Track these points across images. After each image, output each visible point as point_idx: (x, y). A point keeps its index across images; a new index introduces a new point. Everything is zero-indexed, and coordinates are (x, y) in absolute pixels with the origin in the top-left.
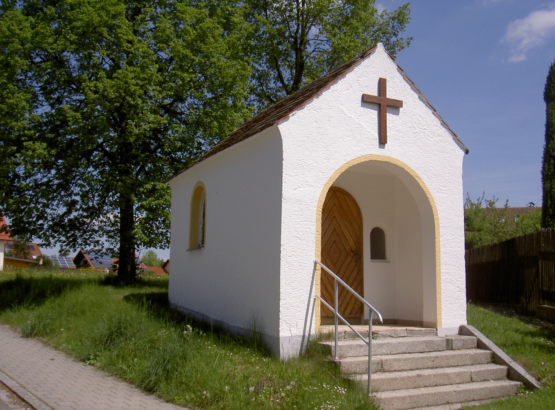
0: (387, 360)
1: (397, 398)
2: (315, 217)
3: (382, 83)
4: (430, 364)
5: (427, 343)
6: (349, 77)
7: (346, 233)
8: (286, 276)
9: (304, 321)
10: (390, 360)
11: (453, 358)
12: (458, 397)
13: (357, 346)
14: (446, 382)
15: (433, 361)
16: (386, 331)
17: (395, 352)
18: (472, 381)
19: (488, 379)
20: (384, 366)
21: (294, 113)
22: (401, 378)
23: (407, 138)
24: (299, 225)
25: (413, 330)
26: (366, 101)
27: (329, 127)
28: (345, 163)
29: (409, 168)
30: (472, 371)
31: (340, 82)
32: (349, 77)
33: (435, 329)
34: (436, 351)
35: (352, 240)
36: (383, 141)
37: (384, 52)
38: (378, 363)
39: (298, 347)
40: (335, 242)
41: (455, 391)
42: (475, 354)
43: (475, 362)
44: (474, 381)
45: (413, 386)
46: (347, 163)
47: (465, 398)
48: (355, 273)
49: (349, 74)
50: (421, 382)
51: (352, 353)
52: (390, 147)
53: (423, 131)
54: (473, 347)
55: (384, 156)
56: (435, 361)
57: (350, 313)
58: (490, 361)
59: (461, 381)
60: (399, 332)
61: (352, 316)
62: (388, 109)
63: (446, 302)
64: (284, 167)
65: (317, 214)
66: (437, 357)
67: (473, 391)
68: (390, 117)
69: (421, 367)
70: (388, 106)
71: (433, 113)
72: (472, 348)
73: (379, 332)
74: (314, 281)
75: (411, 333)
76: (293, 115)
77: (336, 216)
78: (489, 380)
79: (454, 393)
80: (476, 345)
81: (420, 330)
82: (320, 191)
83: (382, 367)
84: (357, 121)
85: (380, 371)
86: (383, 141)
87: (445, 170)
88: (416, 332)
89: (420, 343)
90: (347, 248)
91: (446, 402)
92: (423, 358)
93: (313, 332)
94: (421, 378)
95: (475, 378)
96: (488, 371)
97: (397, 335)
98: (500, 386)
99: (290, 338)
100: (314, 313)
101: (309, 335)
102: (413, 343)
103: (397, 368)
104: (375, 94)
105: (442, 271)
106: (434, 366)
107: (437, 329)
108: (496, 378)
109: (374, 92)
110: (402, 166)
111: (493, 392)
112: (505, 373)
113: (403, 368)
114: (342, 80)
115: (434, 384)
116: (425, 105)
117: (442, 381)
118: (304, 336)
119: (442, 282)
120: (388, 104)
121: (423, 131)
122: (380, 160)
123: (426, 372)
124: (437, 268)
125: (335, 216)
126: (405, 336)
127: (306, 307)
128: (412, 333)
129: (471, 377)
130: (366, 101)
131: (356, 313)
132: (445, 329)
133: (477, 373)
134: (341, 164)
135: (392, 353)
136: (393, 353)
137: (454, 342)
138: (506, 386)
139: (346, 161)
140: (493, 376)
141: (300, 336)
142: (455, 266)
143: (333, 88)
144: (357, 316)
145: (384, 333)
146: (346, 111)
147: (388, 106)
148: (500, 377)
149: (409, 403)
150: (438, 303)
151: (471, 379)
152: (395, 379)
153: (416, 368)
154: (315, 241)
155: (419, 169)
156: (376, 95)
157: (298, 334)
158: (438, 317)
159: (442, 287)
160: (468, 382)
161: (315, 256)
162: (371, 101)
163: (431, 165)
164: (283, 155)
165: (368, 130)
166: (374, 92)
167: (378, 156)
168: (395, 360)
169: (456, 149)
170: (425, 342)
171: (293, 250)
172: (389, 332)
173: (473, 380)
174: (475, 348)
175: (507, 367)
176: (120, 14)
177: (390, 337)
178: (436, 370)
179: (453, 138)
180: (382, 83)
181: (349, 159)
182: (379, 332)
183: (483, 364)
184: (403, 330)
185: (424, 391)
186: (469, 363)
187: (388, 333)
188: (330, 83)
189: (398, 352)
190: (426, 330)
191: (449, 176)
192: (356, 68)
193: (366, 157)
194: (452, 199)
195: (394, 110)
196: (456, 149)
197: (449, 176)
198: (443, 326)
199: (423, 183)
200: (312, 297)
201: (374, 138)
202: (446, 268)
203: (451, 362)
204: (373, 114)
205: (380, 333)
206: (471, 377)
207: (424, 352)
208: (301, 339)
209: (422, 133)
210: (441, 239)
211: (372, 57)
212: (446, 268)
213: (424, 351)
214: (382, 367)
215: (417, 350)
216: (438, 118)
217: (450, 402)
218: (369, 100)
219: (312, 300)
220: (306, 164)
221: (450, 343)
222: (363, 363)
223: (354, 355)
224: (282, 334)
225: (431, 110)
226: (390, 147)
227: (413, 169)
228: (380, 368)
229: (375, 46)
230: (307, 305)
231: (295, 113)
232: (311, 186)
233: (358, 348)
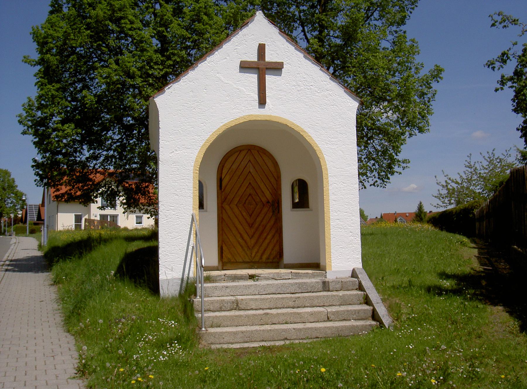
0: (242, 300)
1: (228, 333)
2: (192, 175)
3: (261, 49)
4: (291, 304)
5: (299, 285)
6: (226, 47)
7: (262, 185)
8: (164, 228)
9: (183, 266)
10: (245, 300)
11: (317, 299)
12: (298, 334)
13: (223, 287)
14: (298, 320)
15: (295, 301)
16: (269, 274)
17: (264, 293)
18: (328, 319)
19: (349, 318)
20: (239, 305)
21: (169, 86)
22: (246, 315)
23: (291, 96)
24: (176, 184)
25: (299, 273)
26: (245, 67)
27: (206, 95)
28: (222, 125)
29: (293, 124)
30: (329, 311)
31: (217, 53)
32: (226, 47)
33: (325, 272)
34: (310, 292)
35: (268, 192)
36: (262, 102)
37: (265, 20)
38: (233, 302)
39: (178, 288)
40: (250, 195)
41: (294, 329)
42: (344, 295)
43: (344, 302)
44: (331, 321)
45: (260, 323)
46: (224, 125)
47: (307, 335)
48: (272, 222)
49: (226, 44)
50: (269, 319)
51: (217, 293)
52: (271, 106)
53: (309, 88)
54: (354, 288)
55: (264, 116)
56: (296, 302)
57: (268, 258)
58: (363, 301)
59: (316, 320)
60: (283, 275)
61: (270, 260)
62: (267, 72)
63: (337, 246)
64: (160, 135)
65: (194, 173)
66: (299, 298)
67: (316, 329)
68: (270, 79)
69: (280, 306)
70: (267, 68)
71: (320, 69)
72: (353, 289)
73: (261, 275)
74: (192, 231)
75: (296, 276)
76: (169, 88)
77: (251, 171)
78: (350, 320)
79: (294, 330)
80: (357, 287)
81: (307, 273)
82: (197, 152)
83: (237, 305)
84: (235, 86)
85: (235, 309)
86: (262, 102)
87: (335, 122)
88: (302, 275)
89: (292, 285)
90: (264, 200)
91: (284, 338)
92: (283, 298)
93: (191, 275)
94: (268, 316)
95: (332, 317)
96: (348, 311)
97: (281, 277)
98: (350, 326)
99: (168, 281)
100: (193, 259)
101: (188, 278)
102: (283, 285)
103: (253, 307)
104: (255, 59)
105: (331, 217)
106: (296, 306)
107: (326, 272)
108: (359, 318)
109: (253, 57)
110: (285, 123)
111: (341, 331)
112: (370, 314)
113: (261, 307)
114: (219, 51)
115: (284, 322)
116: (311, 63)
117: (292, 320)
118: (182, 279)
119: (331, 228)
120: (268, 67)
121: (309, 88)
122: (259, 119)
123: (274, 311)
124: (325, 215)
125: (250, 172)
126: (289, 279)
127: (185, 254)
128: (297, 276)
129: (328, 317)
130: (245, 67)
131: (274, 258)
132: (336, 272)
133: (333, 313)
134: (219, 127)
135: (260, 294)
136: (261, 294)
137: (330, 284)
138: (357, 325)
139: (224, 124)
140: (354, 316)
141: (180, 279)
142: (347, 212)
143: (209, 59)
144: (274, 260)
145: (266, 275)
146: (222, 78)
147: (267, 68)
148: (363, 317)
149: (241, 338)
150: (327, 247)
151: (328, 318)
152: (240, 316)
153: (275, 307)
154: (192, 197)
155: (304, 124)
156: (256, 60)
157: (176, 277)
158: (327, 261)
159: (331, 233)
160: (324, 321)
161: (193, 210)
162: (248, 66)
163: (318, 119)
164: (159, 124)
165: (247, 93)
166: (253, 57)
167: (258, 116)
168: (252, 299)
169: (348, 101)
170: (296, 283)
171: (171, 205)
172: (272, 275)
173: (330, 319)
174: (357, 289)
175: (372, 308)
176: (125, 6)
177: (273, 280)
178: (314, 308)
179: (345, 91)
180: (261, 49)
181: (226, 121)
182: (261, 275)
183: (354, 304)
184: (287, 273)
185: (268, 327)
186: (338, 304)
187: (271, 276)
188: (205, 56)
189: (266, 293)
190: (313, 273)
191: (339, 128)
192: (234, 38)
193: (245, 118)
194: (343, 149)
195: (276, 72)
196: (348, 101)
197: (339, 128)
198: (333, 269)
199: (309, 136)
200: (190, 244)
201: (253, 99)
202: (336, 214)
203: (315, 302)
204: (253, 78)
205: (262, 276)
206: (328, 317)
207: (295, 293)
208: (180, 282)
209: (308, 89)
210: (330, 188)
211: (250, 25)
212: (336, 214)
213: (295, 292)
214: (237, 305)
215: (288, 291)
216: (327, 74)
217: (288, 338)
218: (246, 66)
219: (190, 248)
220: (182, 130)
221: (327, 285)
222: (217, 302)
223: (220, 295)
224: (161, 277)
225: (318, 66)
226: (271, 106)
227: (298, 124)
228: (235, 307)
229: (254, 15)
230: (185, 252)
231: (171, 86)
232: (188, 149)
233: (224, 289)
